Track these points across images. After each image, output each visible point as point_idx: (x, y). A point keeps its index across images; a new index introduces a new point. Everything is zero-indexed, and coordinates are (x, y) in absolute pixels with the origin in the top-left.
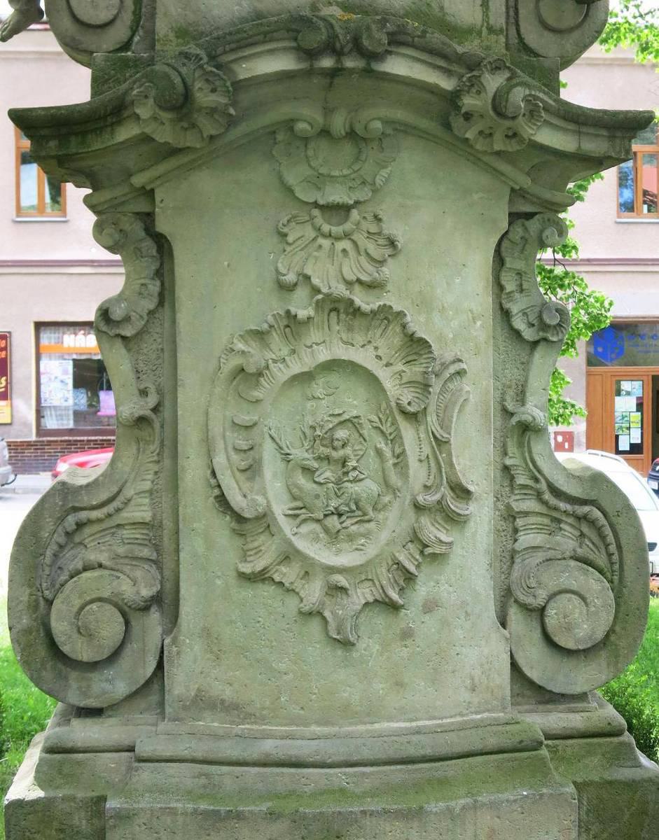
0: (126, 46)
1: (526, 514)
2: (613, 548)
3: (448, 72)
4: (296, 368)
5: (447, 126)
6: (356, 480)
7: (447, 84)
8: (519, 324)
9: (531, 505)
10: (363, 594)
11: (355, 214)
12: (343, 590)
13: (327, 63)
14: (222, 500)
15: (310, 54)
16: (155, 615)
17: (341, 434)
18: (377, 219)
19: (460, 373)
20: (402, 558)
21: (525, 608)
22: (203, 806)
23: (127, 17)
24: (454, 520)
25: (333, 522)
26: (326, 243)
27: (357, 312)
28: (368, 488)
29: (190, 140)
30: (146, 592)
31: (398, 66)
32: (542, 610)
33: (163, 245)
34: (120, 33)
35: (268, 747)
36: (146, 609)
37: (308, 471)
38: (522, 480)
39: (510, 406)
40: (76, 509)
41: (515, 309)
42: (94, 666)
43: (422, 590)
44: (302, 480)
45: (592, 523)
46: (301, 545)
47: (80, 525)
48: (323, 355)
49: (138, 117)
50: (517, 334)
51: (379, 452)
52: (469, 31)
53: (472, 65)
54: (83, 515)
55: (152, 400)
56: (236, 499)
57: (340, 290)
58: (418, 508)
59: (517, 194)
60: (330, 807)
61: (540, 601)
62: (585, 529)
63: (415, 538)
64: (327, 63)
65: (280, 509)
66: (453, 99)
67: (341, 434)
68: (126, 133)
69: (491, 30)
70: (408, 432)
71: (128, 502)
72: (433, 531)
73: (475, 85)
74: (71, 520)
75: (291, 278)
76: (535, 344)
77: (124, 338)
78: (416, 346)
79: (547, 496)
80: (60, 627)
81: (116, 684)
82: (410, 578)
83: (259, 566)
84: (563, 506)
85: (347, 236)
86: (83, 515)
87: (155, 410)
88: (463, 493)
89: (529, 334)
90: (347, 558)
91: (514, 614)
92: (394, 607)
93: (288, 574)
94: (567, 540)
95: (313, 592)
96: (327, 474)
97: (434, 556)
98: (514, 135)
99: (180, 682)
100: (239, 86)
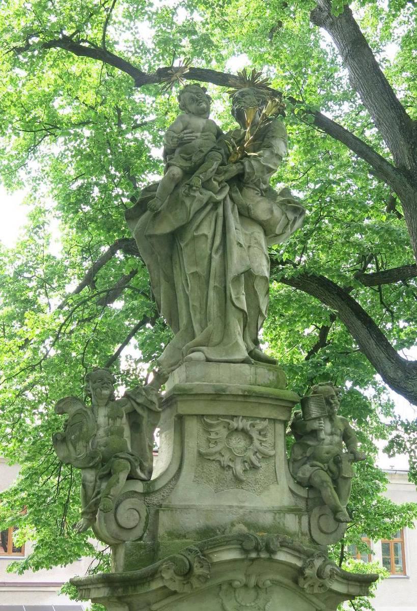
0: (141, 539)
3: (299, 558)
5: (296, 582)
7: (299, 564)
15: (245, 551)
23: (142, 525)
29: (187, 589)
31: (282, 556)
34: (138, 532)
49: (162, 578)
52: (294, 535)
53: (310, 555)
64: (254, 555)
66: (301, 571)
68: (155, 585)
69: (303, 534)
73: (311, 565)
98: (322, 586)
100: (213, 564)
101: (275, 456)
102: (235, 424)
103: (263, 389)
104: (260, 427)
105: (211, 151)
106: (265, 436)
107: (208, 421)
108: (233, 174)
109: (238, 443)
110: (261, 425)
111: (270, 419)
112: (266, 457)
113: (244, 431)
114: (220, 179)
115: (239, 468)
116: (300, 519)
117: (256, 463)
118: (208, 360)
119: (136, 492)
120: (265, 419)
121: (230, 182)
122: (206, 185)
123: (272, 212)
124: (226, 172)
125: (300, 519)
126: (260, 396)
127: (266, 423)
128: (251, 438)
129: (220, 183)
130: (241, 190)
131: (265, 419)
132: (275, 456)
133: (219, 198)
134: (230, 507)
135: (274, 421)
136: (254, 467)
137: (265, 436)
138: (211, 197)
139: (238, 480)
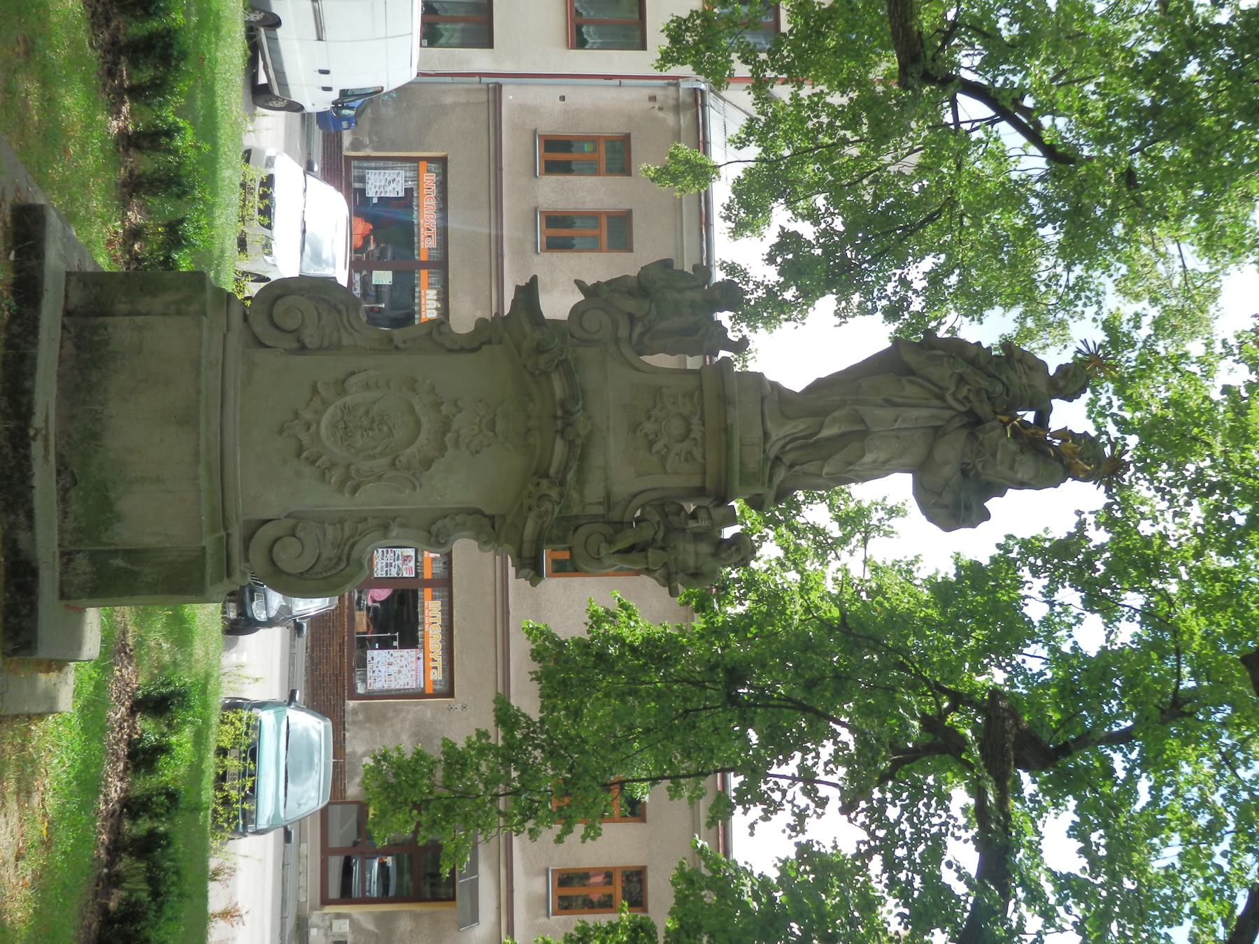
0: (572, 336)
1: (342, 529)
2: (324, 575)
4: (417, 407)
6: (362, 436)
7: (552, 471)
8: (439, 524)
9: (347, 532)
10: (305, 439)
11: (491, 434)
12: (308, 429)
13: (559, 413)
14: (353, 373)
15: (562, 405)
16: (295, 345)
17: (385, 428)
18: (489, 445)
19: (414, 488)
20: (324, 458)
21: (295, 526)
22: (203, 360)
24: (341, 485)
25: (342, 425)
26: (477, 420)
27: (444, 434)
28: (359, 442)
30: (307, 341)
32: (294, 535)
33: (474, 350)
35: (231, 394)
36: (299, 340)
37: (367, 412)
38: (360, 527)
39: (398, 520)
40: (347, 310)
41: (447, 521)
42: (270, 316)
43: (307, 470)
44: (362, 410)
45: (338, 564)
46: (330, 410)
47: (339, 312)
48: (424, 420)
50: (434, 522)
51: (375, 447)
54: (344, 313)
55: (401, 346)
56: (353, 380)
57: (455, 427)
58: (348, 467)
59: (503, 517)
60: (202, 419)
61: (300, 534)
62: (334, 561)
63: (333, 465)
65: (348, 399)
67: (385, 428)
70: (385, 461)
71: (351, 335)
72: (335, 477)
74: (341, 307)
75: (460, 404)
76: (429, 532)
77: (430, 333)
78: (427, 464)
79: (352, 540)
80: (290, 300)
81: (260, 327)
82: (313, 462)
83: (321, 390)
84: (346, 549)
85: (481, 431)
86: (344, 313)
87: (397, 348)
88: (355, 490)
89: (434, 529)
90: (323, 431)
91: (292, 522)
92: (298, 455)
93: (316, 404)
94: (329, 552)
95: (307, 415)
96: (366, 422)
97: (323, 475)
99: (260, 355)
101: (666, 472)
102: (695, 420)
103: (736, 460)
104: (695, 453)
105: (1004, 384)
106: (686, 460)
107: (696, 395)
108: (980, 412)
109: (676, 427)
110: (697, 453)
111: (704, 466)
112: (663, 460)
113: (689, 431)
114: (971, 397)
115: (649, 427)
116: (600, 503)
117: (656, 447)
118: (763, 399)
119: (617, 329)
120: (704, 458)
121: (971, 412)
122: (961, 380)
123: (946, 464)
124: (981, 401)
125: (600, 503)
126: (729, 447)
127: (700, 459)
128: (682, 441)
129: (966, 398)
130: (963, 426)
131: (704, 458)
132: (666, 472)
133: (949, 398)
134: (608, 418)
135: (704, 473)
136: (651, 444)
137: (686, 460)
138: (947, 389)
139: (635, 428)
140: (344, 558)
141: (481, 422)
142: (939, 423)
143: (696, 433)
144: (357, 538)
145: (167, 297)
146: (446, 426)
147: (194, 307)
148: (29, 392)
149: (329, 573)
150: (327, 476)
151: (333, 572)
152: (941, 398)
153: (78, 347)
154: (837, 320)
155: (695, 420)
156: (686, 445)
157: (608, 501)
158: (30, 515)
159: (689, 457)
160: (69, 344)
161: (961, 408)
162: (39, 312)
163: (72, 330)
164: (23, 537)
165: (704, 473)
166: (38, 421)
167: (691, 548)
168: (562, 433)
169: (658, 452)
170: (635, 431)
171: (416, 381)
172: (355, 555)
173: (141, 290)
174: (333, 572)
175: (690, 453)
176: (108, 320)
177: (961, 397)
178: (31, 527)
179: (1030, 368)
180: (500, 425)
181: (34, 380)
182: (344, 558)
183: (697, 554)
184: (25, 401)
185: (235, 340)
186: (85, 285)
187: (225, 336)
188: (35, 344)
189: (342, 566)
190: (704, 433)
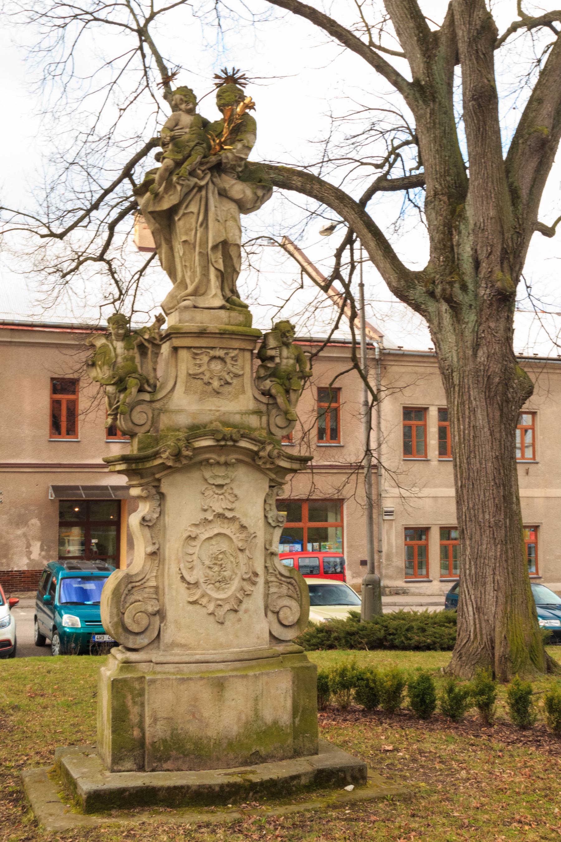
0: (148, 432)
1: (272, 582)
2: (298, 592)
3: (256, 445)
4: (207, 536)
5: (254, 460)
6: (225, 571)
7: (255, 449)
8: (270, 521)
9: (273, 579)
10: (227, 607)
11: (225, 488)
12: (220, 605)
13: (223, 443)
14: (182, 578)
16: (157, 618)
17: (220, 556)
18: (232, 489)
19: (255, 537)
20: (238, 595)
21: (273, 612)
22: (179, 677)
23: (149, 423)
24: (254, 583)
25: (217, 584)
26: (216, 496)
27: (226, 518)
28: (227, 574)
29: (178, 465)
30: (156, 609)
31: (243, 444)
32: (278, 613)
33: (162, 496)
34: (146, 428)
35: (198, 657)
36: (154, 615)
37: (210, 568)
38: (271, 571)
39: (268, 547)
40: (131, 582)
41: (269, 516)
42: (137, 634)
43: (244, 606)
44: (208, 571)
45: (292, 584)
46: (209, 592)
47: (133, 588)
48: (216, 531)
49: (161, 457)
50: (269, 524)
51: (232, 562)
52: (255, 429)
53: (263, 443)
54: (134, 584)
55: (157, 546)
56: (187, 578)
57: (221, 511)
58: (244, 580)
59: (271, 480)
60: (220, 675)
61: (277, 610)
62: (290, 586)
63: (242, 589)
64: (223, 443)
65: (202, 580)
66: (256, 453)
67: (220, 556)
68: (158, 462)
69: (262, 428)
70: (240, 555)
71: (148, 580)
72: (248, 587)
73: (264, 449)
74: (130, 586)
75: (206, 507)
76: (275, 527)
77: (149, 526)
78: (243, 527)
79: (278, 576)
80: (128, 620)
81: (143, 641)
82: (241, 602)
83: (195, 598)
84: (283, 579)
85: (222, 494)
86: (134, 584)
87: (158, 549)
88: (256, 575)
89: (273, 524)
90: (222, 596)
91: (269, 614)
92: (236, 611)
93: (204, 601)
94: (284, 590)
95: (211, 607)
96: (216, 569)
97: (248, 595)
98: (272, 463)
99: (167, 638)
100: (195, 449)
101: (243, 375)
102: (212, 353)
103: (234, 328)
104: (233, 355)
105: (196, 146)
106: (236, 361)
107: (195, 351)
108: (213, 164)
109: (217, 366)
110: (233, 353)
111: (240, 349)
112: (236, 376)
113: (219, 358)
114: (203, 168)
115: (216, 384)
116: (261, 418)
117: (229, 380)
118: (195, 307)
119: (144, 401)
120: (236, 349)
121: (211, 169)
122: (192, 173)
123: (244, 192)
124: (207, 163)
125: (261, 418)
126: (233, 333)
127: (236, 352)
128: (225, 362)
129: (203, 171)
130: (220, 176)
131: (236, 349)
132: (243, 375)
133: (203, 183)
134: (210, 410)
135: (243, 350)
136: (228, 383)
137: (236, 361)
138: (196, 183)
139: (217, 393)
140: (289, 580)
141: (217, 494)
142: (216, 192)
143: (221, 353)
144: (277, 573)
145: (130, 703)
146: (220, 516)
147: (137, 685)
148: (222, 786)
149: (298, 589)
150: (249, 593)
151: (297, 587)
152: (200, 188)
153: (168, 759)
154: (137, 250)
155: (212, 353)
156: (228, 360)
157: (258, 413)
158: (293, 778)
159: (234, 359)
160: (165, 766)
161: (208, 177)
162: (161, 789)
163: (155, 765)
164: (304, 781)
165: (243, 350)
166: (238, 779)
167: (285, 361)
168: (235, 441)
169: (232, 378)
170: (218, 393)
171: (190, 536)
172: (286, 573)
173: (124, 721)
174: (297, 587)
175: (232, 358)
176: (148, 741)
177: (202, 175)
178: (297, 777)
179: (177, 125)
180: (220, 481)
181: (215, 785)
182: (289, 580)
183: (288, 358)
184: (228, 789)
185: (155, 656)
186: (121, 759)
187: (157, 664)
188: (188, 787)
189: (293, 581)
190: (221, 348)
